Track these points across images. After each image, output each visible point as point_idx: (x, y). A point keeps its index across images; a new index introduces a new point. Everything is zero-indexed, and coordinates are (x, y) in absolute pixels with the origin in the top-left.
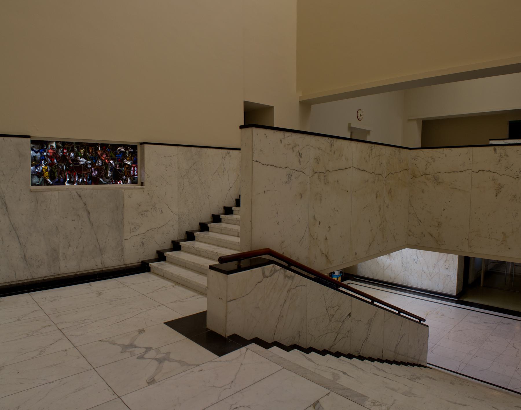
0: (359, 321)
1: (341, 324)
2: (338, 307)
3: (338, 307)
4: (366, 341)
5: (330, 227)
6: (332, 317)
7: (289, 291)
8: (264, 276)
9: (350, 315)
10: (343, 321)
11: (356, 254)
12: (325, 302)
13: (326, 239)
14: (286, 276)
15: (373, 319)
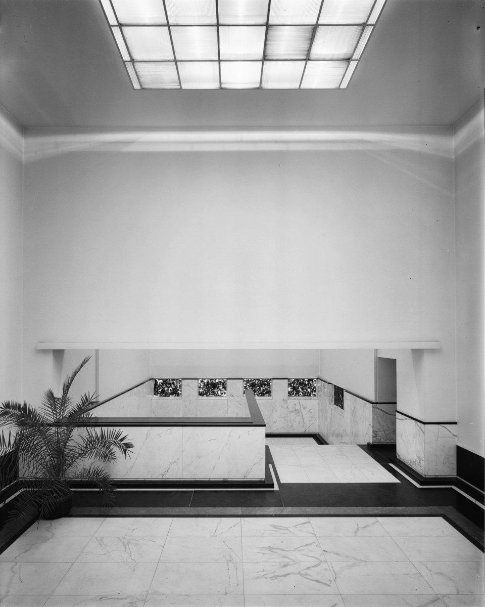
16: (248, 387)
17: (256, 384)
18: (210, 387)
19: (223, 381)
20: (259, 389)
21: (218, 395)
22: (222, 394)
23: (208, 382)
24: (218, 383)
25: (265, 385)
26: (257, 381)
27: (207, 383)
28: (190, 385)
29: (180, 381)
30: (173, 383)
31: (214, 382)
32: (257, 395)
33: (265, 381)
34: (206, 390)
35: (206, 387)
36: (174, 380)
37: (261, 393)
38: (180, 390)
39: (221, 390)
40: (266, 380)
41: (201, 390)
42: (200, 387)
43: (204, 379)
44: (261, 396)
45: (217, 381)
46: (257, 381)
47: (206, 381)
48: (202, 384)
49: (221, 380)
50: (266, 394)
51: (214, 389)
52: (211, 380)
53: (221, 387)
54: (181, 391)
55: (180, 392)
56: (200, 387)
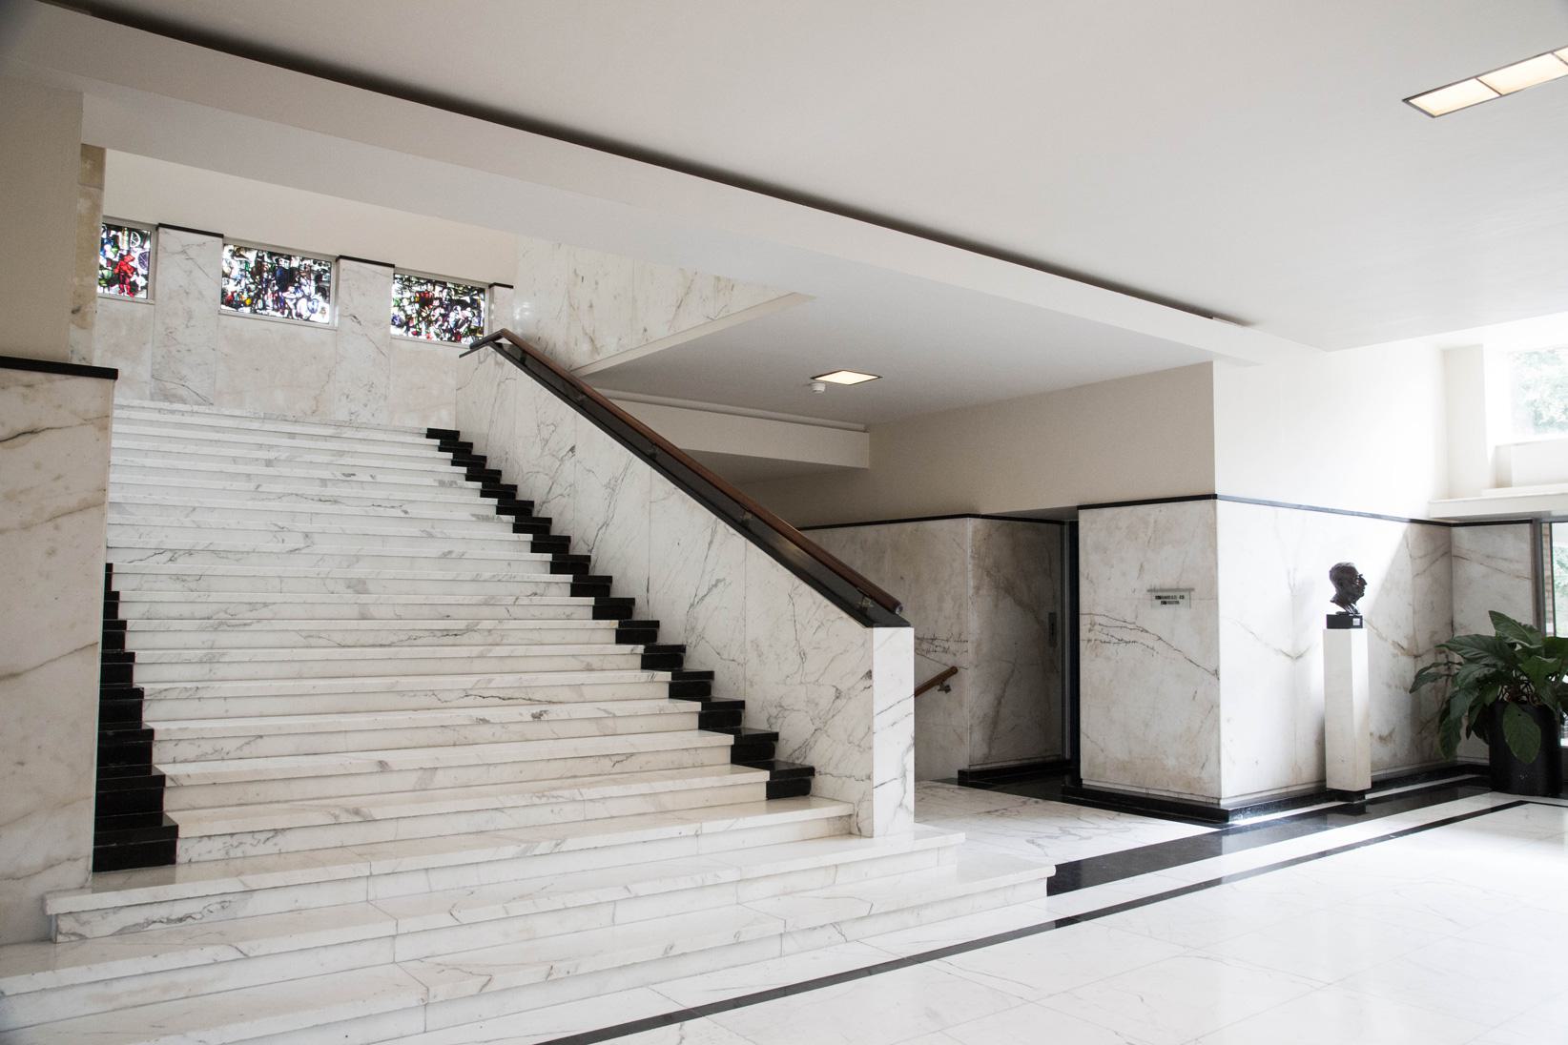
0: (589, 471)
1: (559, 463)
2: (552, 428)
3: (552, 428)
4: (604, 528)
5: (597, 283)
6: (545, 445)
7: (499, 385)
8: (480, 363)
9: (572, 449)
10: (562, 460)
11: (645, 330)
12: (537, 412)
13: (591, 306)
14: (497, 363)
15: (619, 481)
16: (405, 302)
17: (433, 299)
18: (268, 281)
19: (316, 267)
20: (445, 317)
21: (299, 315)
22: (313, 311)
23: (259, 264)
25: (464, 305)
28: (192, 253)
29: (144, 237)
30: (114, 242)
31: (284, 264)
32: (438, 335)
33: (464, 294)
34: (249, 290)
36: (119, 229)
37: (449, 331)
38: (142, 271)
39: (309, 298)
40: (469, 291)
41: (231, 287)
43: (247, 249)
45: (295, 263)
47: (251, 256)
49: (308, 262)
50: (466, 335)
51: (284, 289)
52: (271, 255)
53: (309, 287)
54: (146, 277)
55: (141, 282)
56: (226, 275)
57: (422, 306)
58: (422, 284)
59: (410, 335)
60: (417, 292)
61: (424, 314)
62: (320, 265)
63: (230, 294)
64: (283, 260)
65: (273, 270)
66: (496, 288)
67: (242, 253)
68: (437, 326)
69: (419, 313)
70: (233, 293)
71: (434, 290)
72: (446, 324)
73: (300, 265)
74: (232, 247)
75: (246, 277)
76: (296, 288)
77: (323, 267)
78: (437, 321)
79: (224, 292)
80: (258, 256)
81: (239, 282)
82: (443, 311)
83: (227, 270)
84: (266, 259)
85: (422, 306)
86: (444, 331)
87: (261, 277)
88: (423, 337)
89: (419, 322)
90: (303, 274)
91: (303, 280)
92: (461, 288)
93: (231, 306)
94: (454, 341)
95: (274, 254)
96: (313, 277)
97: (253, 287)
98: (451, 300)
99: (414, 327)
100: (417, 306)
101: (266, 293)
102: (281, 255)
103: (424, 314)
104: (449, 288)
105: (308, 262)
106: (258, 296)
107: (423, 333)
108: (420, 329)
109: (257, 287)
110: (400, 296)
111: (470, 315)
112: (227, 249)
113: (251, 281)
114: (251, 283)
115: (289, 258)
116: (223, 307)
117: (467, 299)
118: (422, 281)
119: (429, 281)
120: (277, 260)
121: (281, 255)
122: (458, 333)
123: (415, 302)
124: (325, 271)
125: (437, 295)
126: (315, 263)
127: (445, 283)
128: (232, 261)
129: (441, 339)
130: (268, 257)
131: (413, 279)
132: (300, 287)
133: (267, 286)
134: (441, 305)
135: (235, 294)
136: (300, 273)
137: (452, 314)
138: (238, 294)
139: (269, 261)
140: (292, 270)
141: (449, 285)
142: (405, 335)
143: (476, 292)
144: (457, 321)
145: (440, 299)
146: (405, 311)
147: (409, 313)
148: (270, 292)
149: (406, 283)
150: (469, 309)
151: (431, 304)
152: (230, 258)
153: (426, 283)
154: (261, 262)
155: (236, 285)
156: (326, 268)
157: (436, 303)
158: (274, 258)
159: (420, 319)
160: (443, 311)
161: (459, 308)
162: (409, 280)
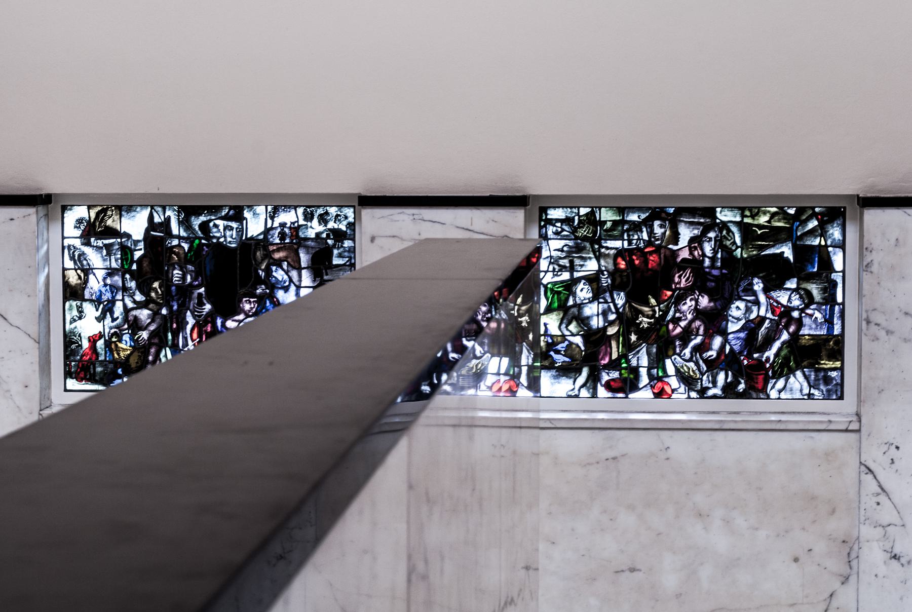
16: (583, 292)
17: (671, 263)
18: (185, 291)
19: (314, 228)
24: (262, 243)
26: (686, 233)
27: (148, 238)
32: (687, 380)
33: (775, 235)
34: (135, 326)
35: (144, 288)
37: (727, 361)
42: (73, 293)
43: (124, 208)
44: (729, 391)
45: (255, 226)
46: (686, 233)
48: (95, 258)
49: (287, 217)
50: (784, 369)
52: (188, 211)
57: (637, 296)
58: (636, 227)
59: (602, 392)
60: (620, 253)
61: (645, 322)
62: (323, 219)
63: (86, 344)
64: (221, 223)
65: (195, 257)
66: (872, 216)
67: (109, 222)
68: (687, 352)
69: (627, 321)
70: (93, 340)
71: (675, 238)
72: (717, 341)
73: (267, 231)
74: (81, 212)
75: (125, 289)
76: (261, 300)
77: (331, 225)
78: (686, 336)
79: (70, 340)
80: (152, 225)
81: (108, 309)
82: (704, 301)
83: (73, 278)
84: (175, 228)
85: (637, 296)
86: (712, 365)
87: (167, 283)
88: (645, 394)
89: (629, 347)
90: (277, 256)
91: (279, 274)
92: (763, 219)
93: (92, 379)
94: (744, 395)
95: (197, 210)
96: (304, 258)
97: (144, 314)
98: (729, 259)
99: (614, 365)
100: (620, 299)
101: (182, 324)
102: (214, 210)
103: (645, 322)
104: (724, 225)
105: (287, 217)
106: (159, 339)
107: (644, 380)
108: (635, 371)
109: (155, 314)
110: (566, 276)
111: (796, 302)
112: (71, 217)
113: (139, 297)
114: (140, 305)
115: (237, 215)
116: (72, 384)
117: (787, 251)
118: (634, 217)
119: (657, 213)
120: (204, 226)
121: (214, 210)
122: (760, 364)
123: (612, 288)
124: (339, 236)
125: (685, 254)
126: (309, 217)
127: (710, 212)
128: (87, 250)
129: (702, 393)
130: (180, 223)
131: (607, 216)
132: (272, 297)
133: (183, 307)
134: (701, 283)
135: (100, 344)
136: (268, 255)
137: (737, 309)
138: (108, 344)
139: (183, 234)
140: (249, 246)
141: (724, 216)
142: (584, 393)
143: (813, 224)
144: (751, 328)
145: (695, 264)
146: (583, 321)
147: (597, 323)
148: (191, 321)
149: (582, 232)
150: (792, 284)
151: (668, 283)
152: (77, 243)
153: (648, 223)
154: (161, 240)
155: (100, 319)
156: (344, 229)
157: (682, 280)
158: (196, 222)
159: (633, 338)
160: (704, 301)
161: (758, 286)
162: (591, 220)
